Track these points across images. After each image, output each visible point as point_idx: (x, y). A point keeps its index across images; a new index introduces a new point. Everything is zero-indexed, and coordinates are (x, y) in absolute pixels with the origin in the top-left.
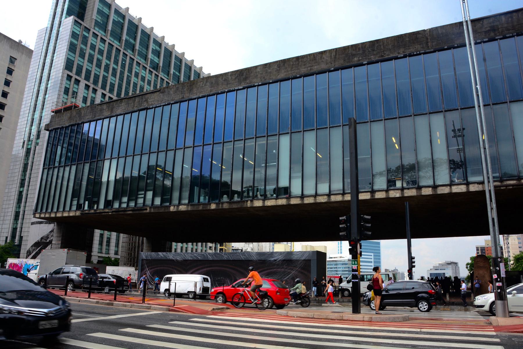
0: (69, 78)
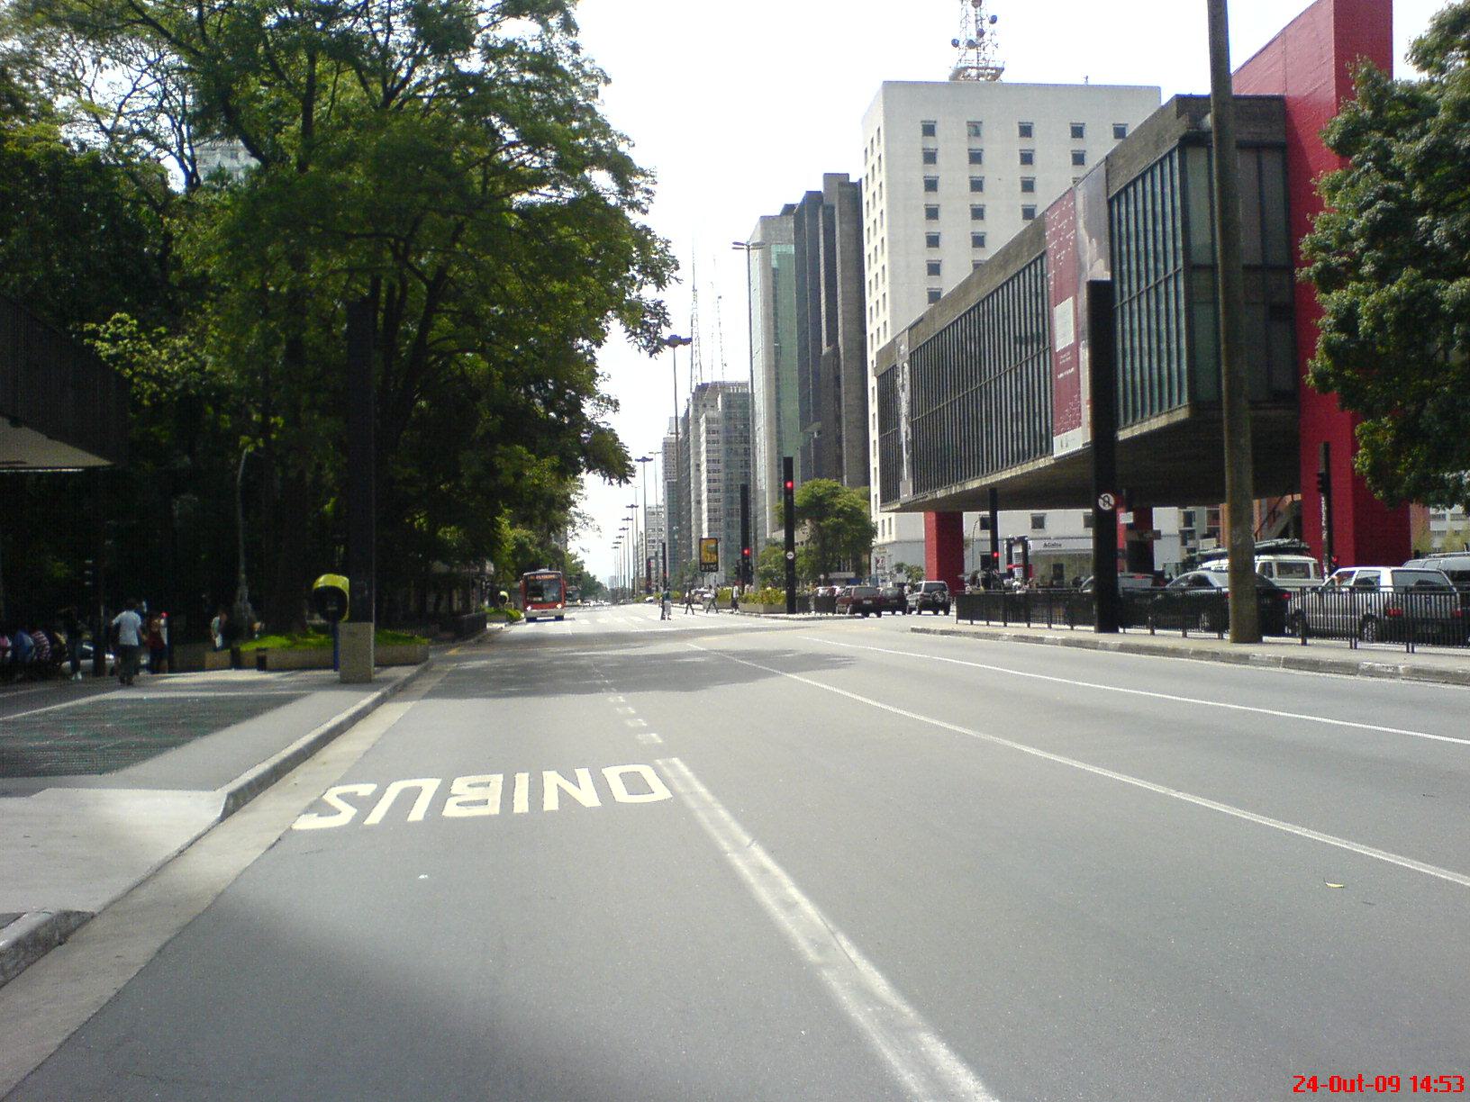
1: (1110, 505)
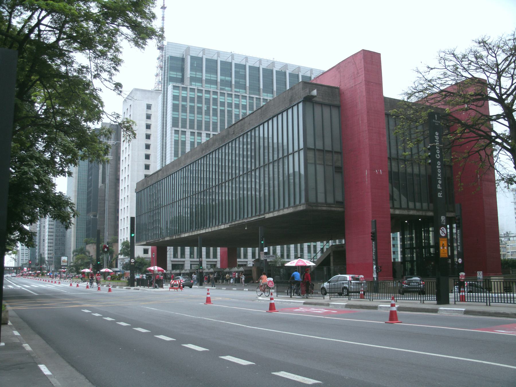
0: (177, 132)
1: (444, 233)
